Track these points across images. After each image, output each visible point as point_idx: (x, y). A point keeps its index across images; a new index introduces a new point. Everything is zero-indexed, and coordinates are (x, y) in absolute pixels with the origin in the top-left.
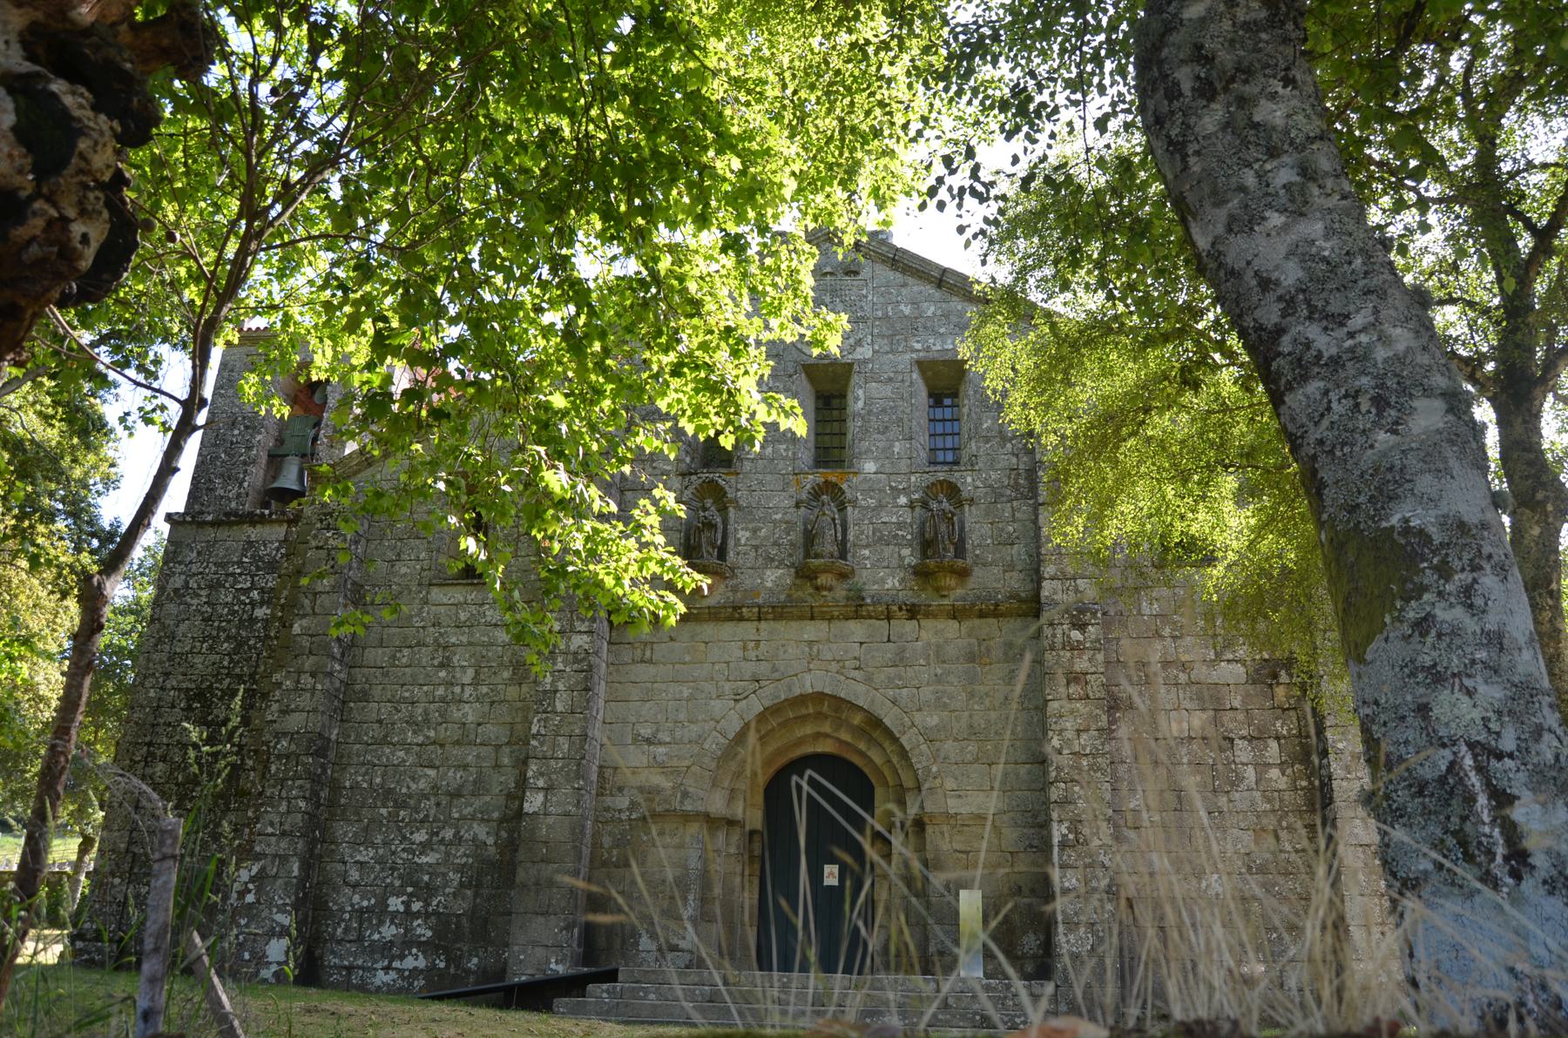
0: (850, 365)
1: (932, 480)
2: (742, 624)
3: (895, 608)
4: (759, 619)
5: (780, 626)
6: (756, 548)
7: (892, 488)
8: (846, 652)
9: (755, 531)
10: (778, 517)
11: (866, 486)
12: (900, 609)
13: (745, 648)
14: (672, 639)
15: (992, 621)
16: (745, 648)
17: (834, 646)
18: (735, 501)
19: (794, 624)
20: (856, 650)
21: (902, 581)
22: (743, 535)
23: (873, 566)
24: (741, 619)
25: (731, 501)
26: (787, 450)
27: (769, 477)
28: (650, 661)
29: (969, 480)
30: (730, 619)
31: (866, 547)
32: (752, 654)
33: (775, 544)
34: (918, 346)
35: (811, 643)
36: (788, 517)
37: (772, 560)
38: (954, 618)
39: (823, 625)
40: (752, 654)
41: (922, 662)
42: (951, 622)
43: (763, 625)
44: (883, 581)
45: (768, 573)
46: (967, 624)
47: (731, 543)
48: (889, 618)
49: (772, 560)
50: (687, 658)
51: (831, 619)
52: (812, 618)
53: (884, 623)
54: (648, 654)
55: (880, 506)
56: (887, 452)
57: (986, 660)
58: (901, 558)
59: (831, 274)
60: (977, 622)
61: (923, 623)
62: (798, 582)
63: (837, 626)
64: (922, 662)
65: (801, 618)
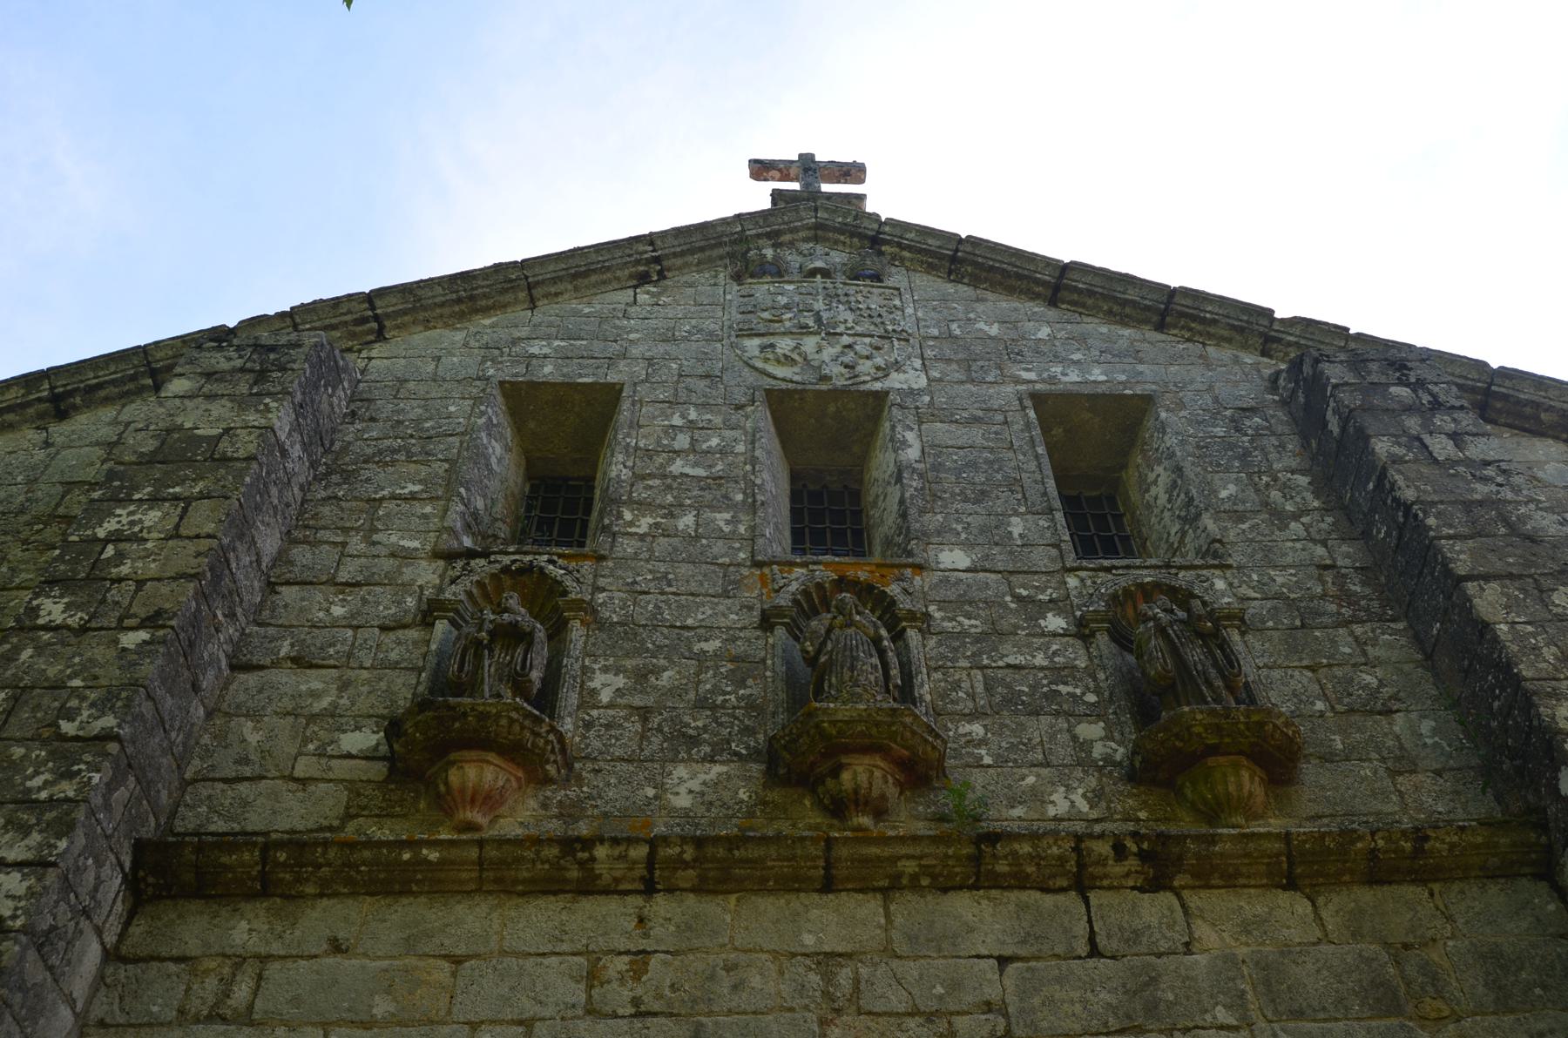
0: (881, 396)
1: (1123, 582)
2: (588, 905)
3: (1103, 848)
4: (649, 888)
5: (721, 910)
6: (644, 713)
7: (1018, 599)
8: (955, 986)
9: (641, 676)
10: (712, 646)
11: (951, 594)
12: (1120, 851)
13: (592, 977)
14: (337, 947)
15: (1410, 891)
16: (592, 977)
17: (911, 970)
18: (588, 610)
19: (769, 906)
20: (989, 983)
21: (1095, 797)
22: (606, 684)
23: (1000, 761)
24: (588, 887)
25: (579, 605)
26: (734, 521)
27: (684, 569)
28: (247, 1018)
29: (1220, 585)
30: (549, 886)
31: (973, 716)
32: (619, 996)
33: (701, 704)
34: (1025, 375)
35: (827, 960)
36: (740, 648)
37: (694, 741)
38: (1291, 885)
39: (870, 907)
40: (619, 996)
41: (1222, 1015)
42: (1284, 898)
43: (661, 905)
44: (1038, 797)
45: (681, 771)
46: (1335, 906)
47: (569, 698)
48: (1082, 885)
49: (694, 741)
50: (382, 1007)
51: (890, 889)
52: (828, 886)
53: (1071, 900)
54: (242, 992)
55: (994, 634)
56: (994, 534)
57: (1430, 1006)
58: (1085, 746)
59: (826, 273)
60: (1366, 896)
61: (1194, 900)
62: (774, 795)
63: (910, 910)
64: (1222, 1015)
65: (792, 884)
